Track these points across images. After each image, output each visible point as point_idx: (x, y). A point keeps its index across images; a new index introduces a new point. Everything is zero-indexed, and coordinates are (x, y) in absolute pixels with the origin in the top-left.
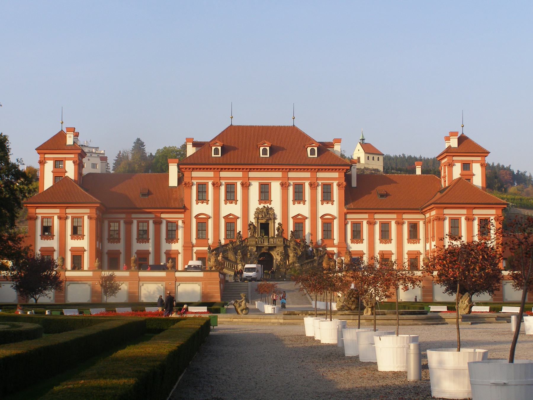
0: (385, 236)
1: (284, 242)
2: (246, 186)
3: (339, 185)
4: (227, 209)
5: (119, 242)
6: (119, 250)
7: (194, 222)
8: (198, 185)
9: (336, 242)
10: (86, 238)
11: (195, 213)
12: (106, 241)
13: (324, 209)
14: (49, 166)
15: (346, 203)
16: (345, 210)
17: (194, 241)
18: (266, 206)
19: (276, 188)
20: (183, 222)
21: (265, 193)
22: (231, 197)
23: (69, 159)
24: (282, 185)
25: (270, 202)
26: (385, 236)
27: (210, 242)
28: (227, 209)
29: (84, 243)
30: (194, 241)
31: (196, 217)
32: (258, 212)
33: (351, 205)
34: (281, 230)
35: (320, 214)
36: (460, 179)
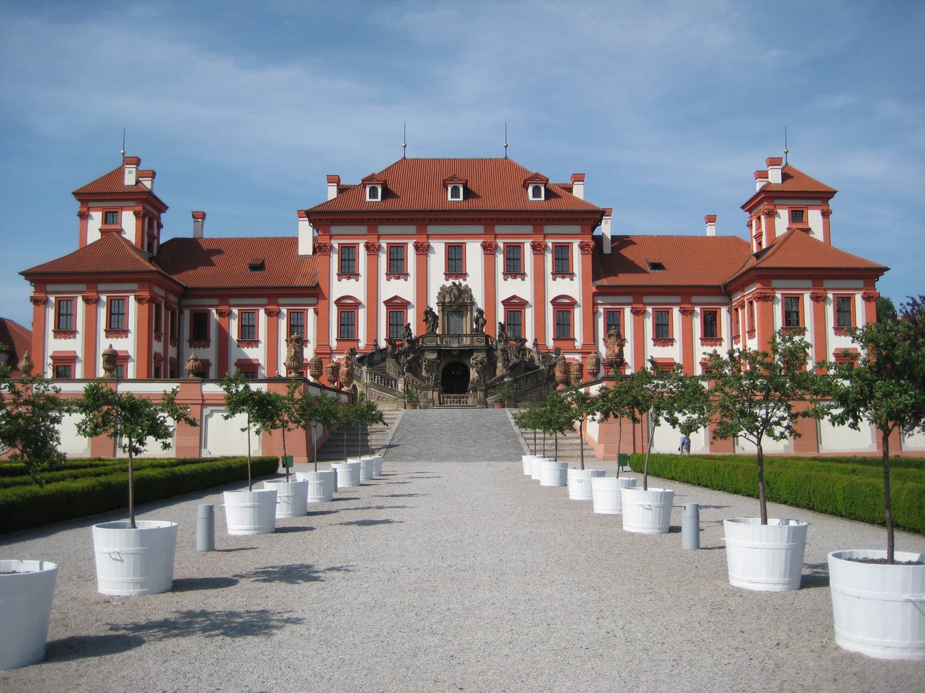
0: (663, 336)
1: (487, 342)
2: (423, 250)
3: (582, 247)
4: (389, 289)
5: (208, 346)
6: (208, 360)
7: (334, 310)
8: (343, 247)
9: (578, 344)
10: (132, 336)
11: (335, 296)
12: (186, 344)
13: (557, 287)
14: (96, 219)
15: (596, 277)
16: (594, 290)
17: (334, 344)
18: (457, 283)
19: (474, 251)
20: (316, 312)
21: (455, 263)
22: (397, 270)
23: (128, 208)
24: (485, 247)
25: (464, 275)
26: (663, 336)
27: (362, 345)
28: (389, 289)
29: (127, 345)
30: (334, 344)
31: (338, 302)
32: (444, 291)
33: (605, 282)
34: (481, 319)
35: (550, 296)
36: (786, 238)
